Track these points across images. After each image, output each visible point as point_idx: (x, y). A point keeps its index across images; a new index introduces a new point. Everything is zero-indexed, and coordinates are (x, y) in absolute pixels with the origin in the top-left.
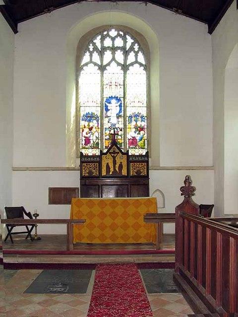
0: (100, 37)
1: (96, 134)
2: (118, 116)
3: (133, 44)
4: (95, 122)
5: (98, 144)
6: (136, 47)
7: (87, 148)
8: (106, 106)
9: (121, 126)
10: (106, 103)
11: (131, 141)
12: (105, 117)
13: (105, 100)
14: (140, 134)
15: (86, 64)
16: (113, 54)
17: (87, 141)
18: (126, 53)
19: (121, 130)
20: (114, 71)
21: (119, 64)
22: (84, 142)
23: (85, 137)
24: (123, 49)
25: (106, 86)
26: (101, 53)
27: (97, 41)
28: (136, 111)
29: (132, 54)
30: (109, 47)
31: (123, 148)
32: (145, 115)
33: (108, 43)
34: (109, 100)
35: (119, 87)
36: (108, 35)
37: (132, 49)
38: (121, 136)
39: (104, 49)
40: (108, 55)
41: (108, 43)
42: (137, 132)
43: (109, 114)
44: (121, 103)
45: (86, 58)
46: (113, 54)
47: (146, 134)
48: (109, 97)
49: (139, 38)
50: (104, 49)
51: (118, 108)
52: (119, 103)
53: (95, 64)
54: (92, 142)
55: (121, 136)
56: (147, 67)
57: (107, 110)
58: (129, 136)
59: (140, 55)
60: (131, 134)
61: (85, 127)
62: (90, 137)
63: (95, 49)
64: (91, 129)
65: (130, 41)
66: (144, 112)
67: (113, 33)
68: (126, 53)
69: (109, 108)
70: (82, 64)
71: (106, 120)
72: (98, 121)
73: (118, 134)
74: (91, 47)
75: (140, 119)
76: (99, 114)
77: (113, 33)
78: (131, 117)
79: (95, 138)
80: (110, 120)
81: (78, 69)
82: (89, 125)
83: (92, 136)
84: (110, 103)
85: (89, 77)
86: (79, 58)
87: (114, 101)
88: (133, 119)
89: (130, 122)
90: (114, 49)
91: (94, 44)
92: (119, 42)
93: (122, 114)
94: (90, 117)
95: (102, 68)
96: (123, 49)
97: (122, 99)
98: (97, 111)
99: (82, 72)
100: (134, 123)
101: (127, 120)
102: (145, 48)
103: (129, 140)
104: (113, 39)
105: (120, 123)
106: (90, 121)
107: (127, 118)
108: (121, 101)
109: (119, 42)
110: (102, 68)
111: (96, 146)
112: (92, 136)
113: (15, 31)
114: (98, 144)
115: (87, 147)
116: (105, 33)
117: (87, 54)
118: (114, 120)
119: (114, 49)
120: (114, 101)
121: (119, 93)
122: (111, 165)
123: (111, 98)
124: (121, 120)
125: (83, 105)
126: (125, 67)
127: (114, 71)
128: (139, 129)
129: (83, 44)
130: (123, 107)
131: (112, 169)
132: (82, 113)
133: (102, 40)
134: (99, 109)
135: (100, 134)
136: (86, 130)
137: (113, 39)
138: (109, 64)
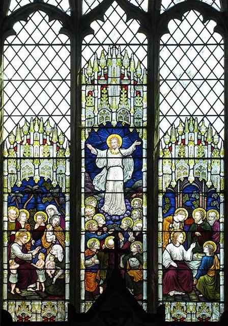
1: (57, 250)
2: (130, 190)
4: (52, 209)
5: (61, 281)
7: (24, 299)
8: (91, 159)
9: (140, 225)
10: (90, 146)
11: (171, 273)
12: (87, 195)
13: (85, 134)
14: (202, 252)
17: (27, 272)
19: (139, 238)
22: (13, 280)
23: (18, 260)
25: (90, 88)
28: (188, 172)
31: (145, 298)
32: (219, 186)
34: (99, 137)
35: (131, 90)
38: (139, 256)
42: (193, 246)
44: (139, 148)
47: (222, 251)
48: (101, 127)
52: (132, 148)
54: (41, 279)
55: (139, 256)
57: (93, 171)
58: (165, 259)
60: (174, 251)
61: (18, 227)
62: (35, 259)
64: (38, 234)
69: (100, 164)
71: (88, 207)
72: (61, 208)
73: (128, 252)
75: (202, 200)
76: (65, 185)
78: (171, 193)
79: (50, 263)
80: (101, 202)
82: (31, 221)
83: (41, 256)
84: (103, 146)
87: (114, 140)
88: (179, 199)
89: (170, 211)
97: (143, 133)
98: (55, 172)
100: (180, 216)
101: (160, 203)
103: (165, 270)
105: (136, 213)
106: (34, 208)
107: (161, 197)
108: (143, 141)
111: (53, 292)
112: (41, 256)
114: (61, 281)
115: (24, 293)
118: (116, 205)
120: (114, 140)
121: (134, 107)
123: (107, 129)
124: (141, 203)
125: (13, 154)
128: (197, 235)
130: (147, 158)
134: (65, 168)
135: (67, 249)
136: (26, 238)
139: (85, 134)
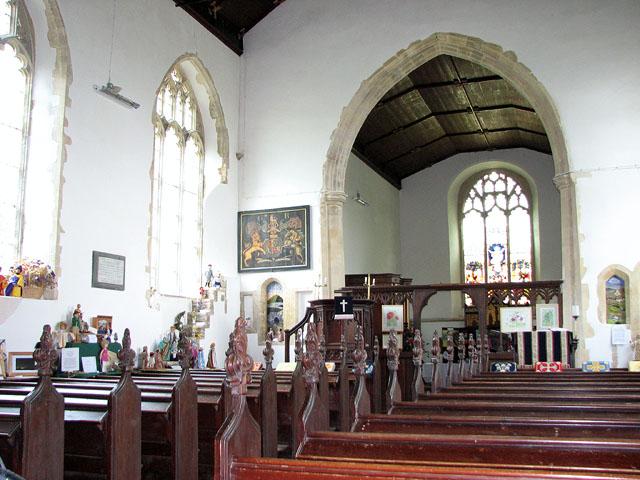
0: (480, 181)
3: (515, 187)
4: (479, 270)
6: (518, 189)
8: (490, 254)
15: (468, 212)
16: (495, 198)
18: (508, 197)
20: (496, 218)
21: (501, 209)
24: (505, 193)
26: (483, 199)
27: (478, 186)
29: (514, 197)
30: (490, 193)
33: (489, 187)
36: (488, 179)
37: (513, 192)
39: (485, 194)
40: (489, 199)
41: (489, 187)
43: (492, 261)
45: (468, 205)
46: (495, 198)
49: (520, 180)
50: (485, 194)
51: (502, 255)
53: (478, 211)
56: (530, 211)
59: (523, 197)
63: (477, 195)
65: (511, 182)
66: (528, 259)
67: (494, 176)
68: (508, 197)
70: (464, 211)
71: (489, 268)
74: (472, 193)
77: (494, 176)
78: (515, 264)
81: (460, 216)
85: (472, 223)
86: (460, 206)
87: (497, 248)
90: (495, 194)
91: (475, 189)
92: (500, 186)
93: (506, 261)
94: (474, 266)
95: (485, 215)
96: (505, 193)
97: (505, 246)
99: (464, 220)
102: (527, 191)
104: (494, 183)
106: (474, 270)
109: (500, 186)
110: (485, 215)
113: (399, 186)
116: (486, 177)
117: (469, 200)
118: (498, 268)
119: (495, 194)
120: (497, 248)
122: (494, 315)
123: (495, 245)
124: (505, 267)
126: (507, 213)
127: (496, 218)
129: (463, 194)
131: (494, 320)
132: (467, 261)
133: (484, 182)
137: (494, 183)
138: (491, 210)
139: (488, 247)
